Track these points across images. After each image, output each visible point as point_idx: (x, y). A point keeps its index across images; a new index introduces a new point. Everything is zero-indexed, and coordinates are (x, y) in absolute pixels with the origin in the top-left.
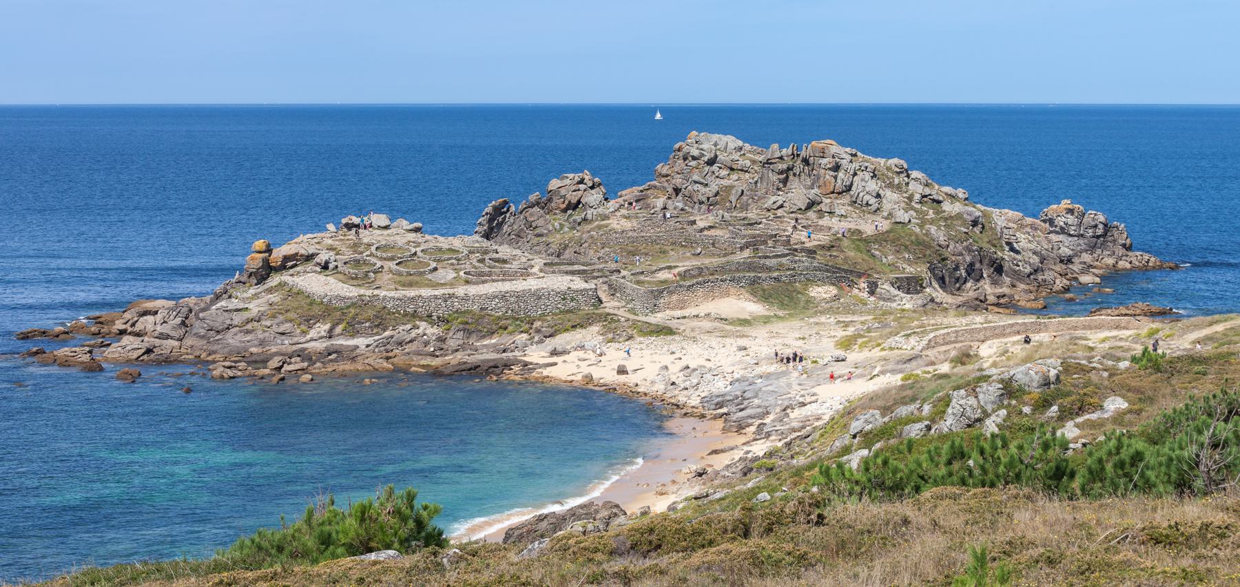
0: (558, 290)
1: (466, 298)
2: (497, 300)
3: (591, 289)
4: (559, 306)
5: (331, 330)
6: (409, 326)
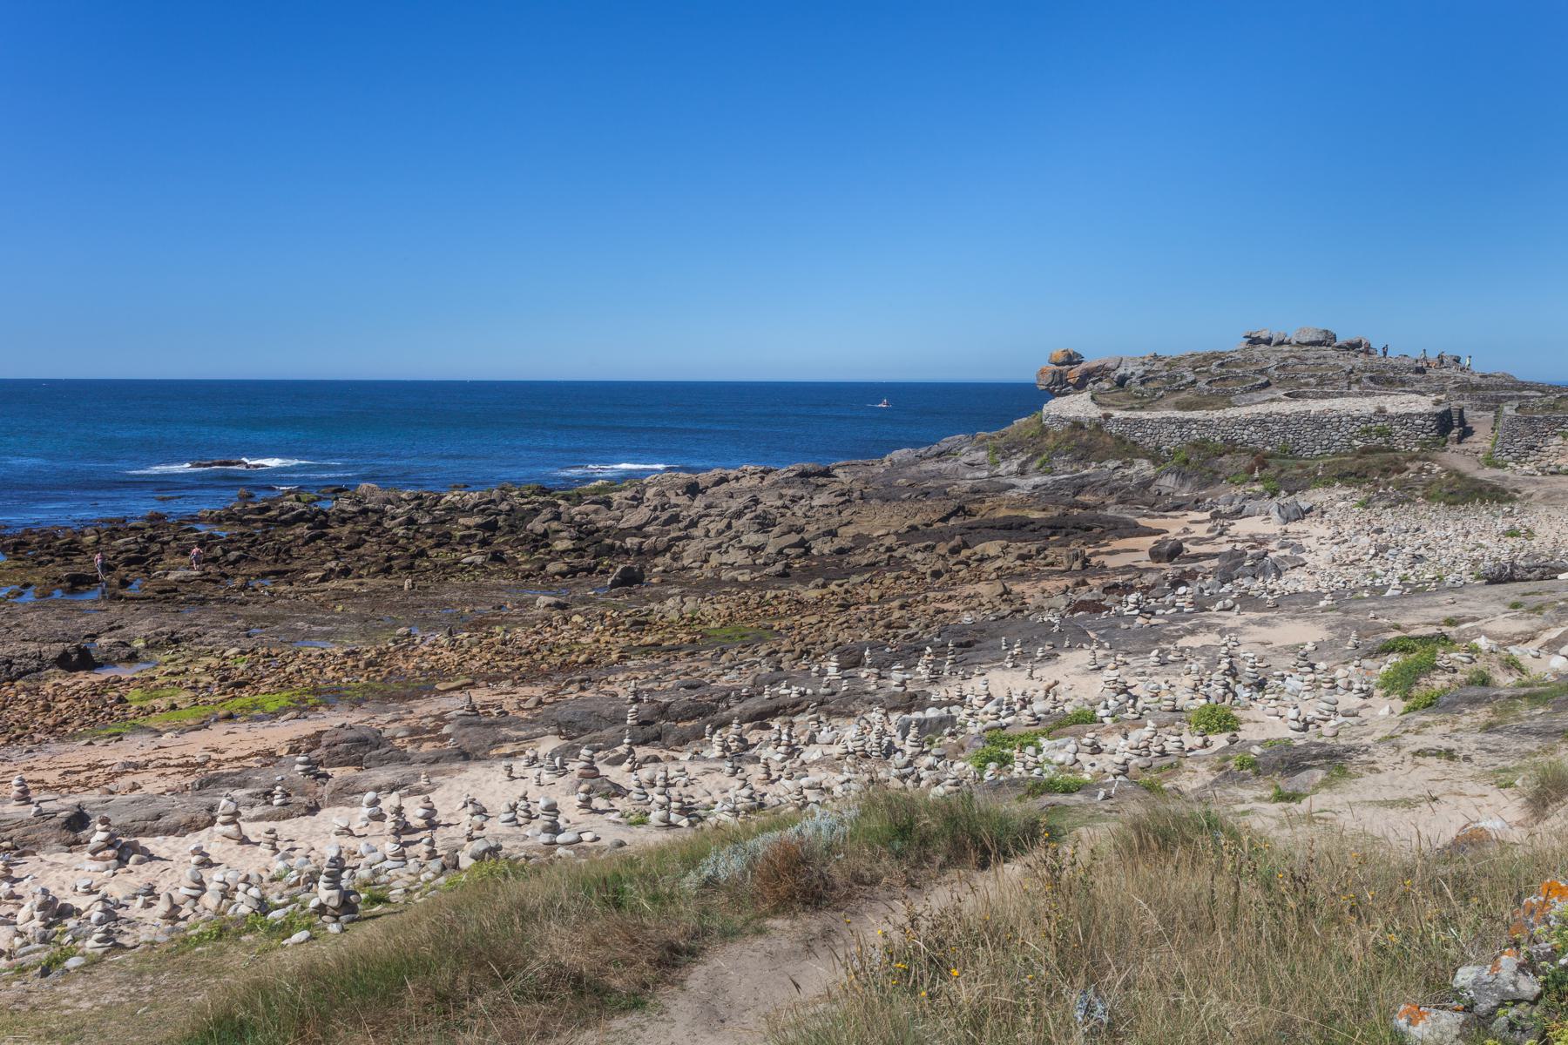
0: (1356, 414)
1: (1207, 424)
2: (1252, 428)
3: (1420, 415)
4: (1355, 442)
5: (1023, 465)
6: (1119, 463)
